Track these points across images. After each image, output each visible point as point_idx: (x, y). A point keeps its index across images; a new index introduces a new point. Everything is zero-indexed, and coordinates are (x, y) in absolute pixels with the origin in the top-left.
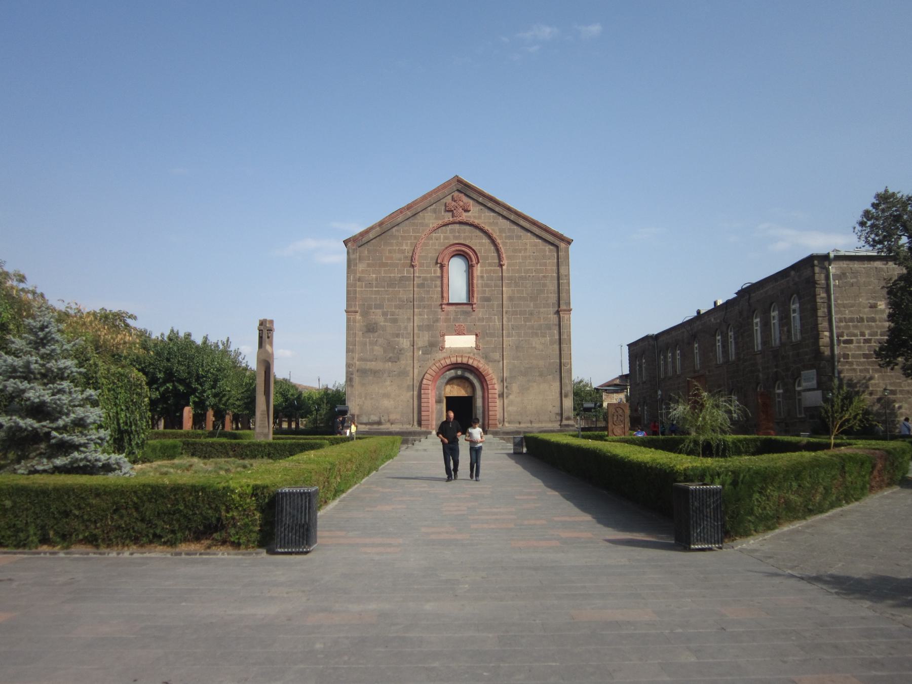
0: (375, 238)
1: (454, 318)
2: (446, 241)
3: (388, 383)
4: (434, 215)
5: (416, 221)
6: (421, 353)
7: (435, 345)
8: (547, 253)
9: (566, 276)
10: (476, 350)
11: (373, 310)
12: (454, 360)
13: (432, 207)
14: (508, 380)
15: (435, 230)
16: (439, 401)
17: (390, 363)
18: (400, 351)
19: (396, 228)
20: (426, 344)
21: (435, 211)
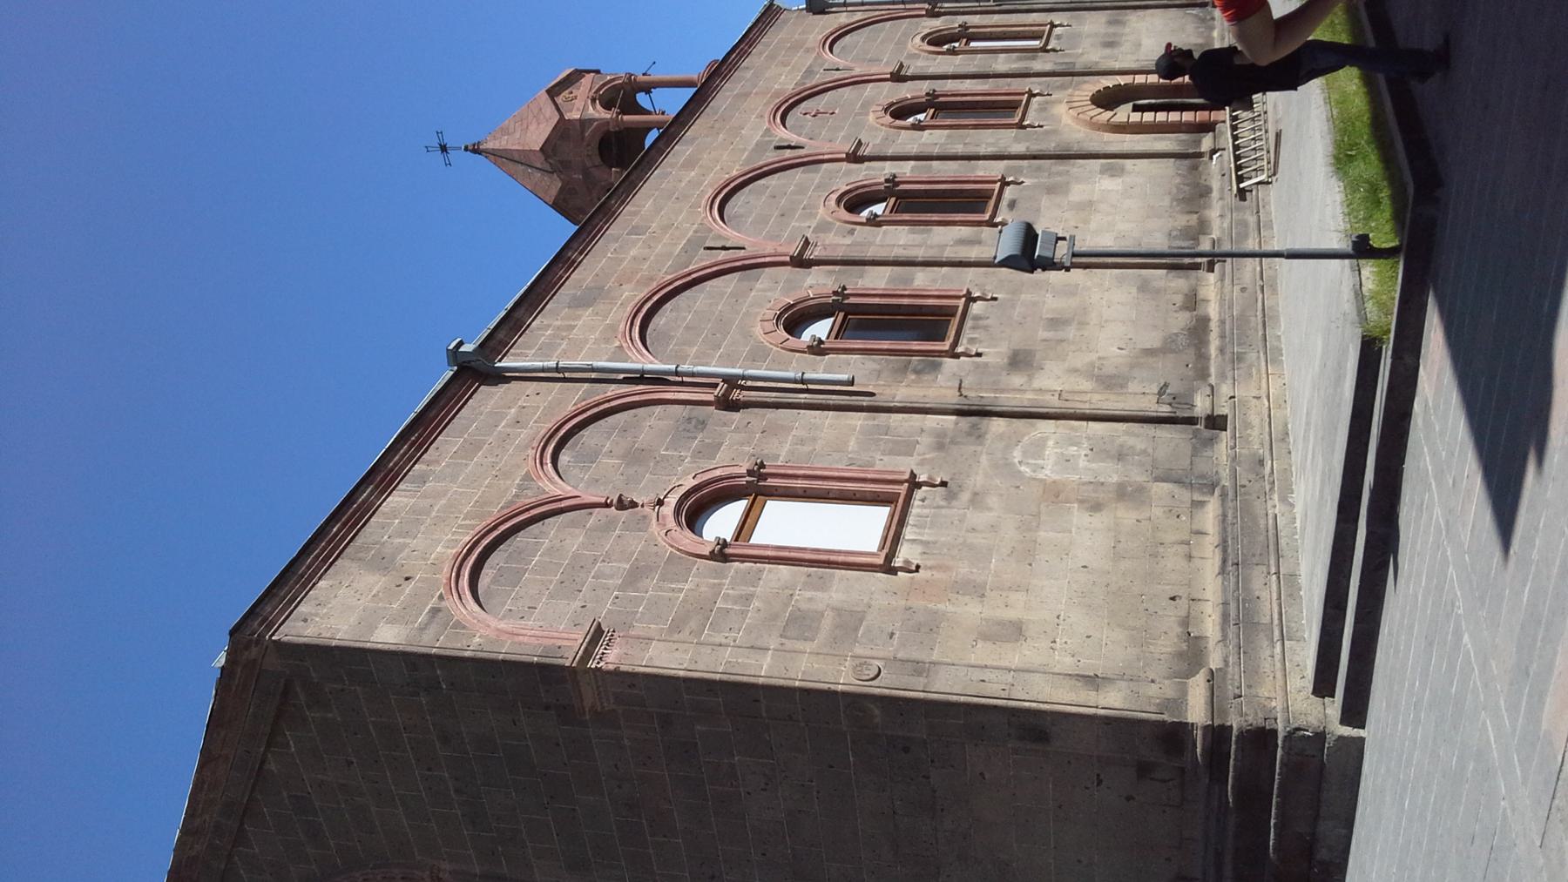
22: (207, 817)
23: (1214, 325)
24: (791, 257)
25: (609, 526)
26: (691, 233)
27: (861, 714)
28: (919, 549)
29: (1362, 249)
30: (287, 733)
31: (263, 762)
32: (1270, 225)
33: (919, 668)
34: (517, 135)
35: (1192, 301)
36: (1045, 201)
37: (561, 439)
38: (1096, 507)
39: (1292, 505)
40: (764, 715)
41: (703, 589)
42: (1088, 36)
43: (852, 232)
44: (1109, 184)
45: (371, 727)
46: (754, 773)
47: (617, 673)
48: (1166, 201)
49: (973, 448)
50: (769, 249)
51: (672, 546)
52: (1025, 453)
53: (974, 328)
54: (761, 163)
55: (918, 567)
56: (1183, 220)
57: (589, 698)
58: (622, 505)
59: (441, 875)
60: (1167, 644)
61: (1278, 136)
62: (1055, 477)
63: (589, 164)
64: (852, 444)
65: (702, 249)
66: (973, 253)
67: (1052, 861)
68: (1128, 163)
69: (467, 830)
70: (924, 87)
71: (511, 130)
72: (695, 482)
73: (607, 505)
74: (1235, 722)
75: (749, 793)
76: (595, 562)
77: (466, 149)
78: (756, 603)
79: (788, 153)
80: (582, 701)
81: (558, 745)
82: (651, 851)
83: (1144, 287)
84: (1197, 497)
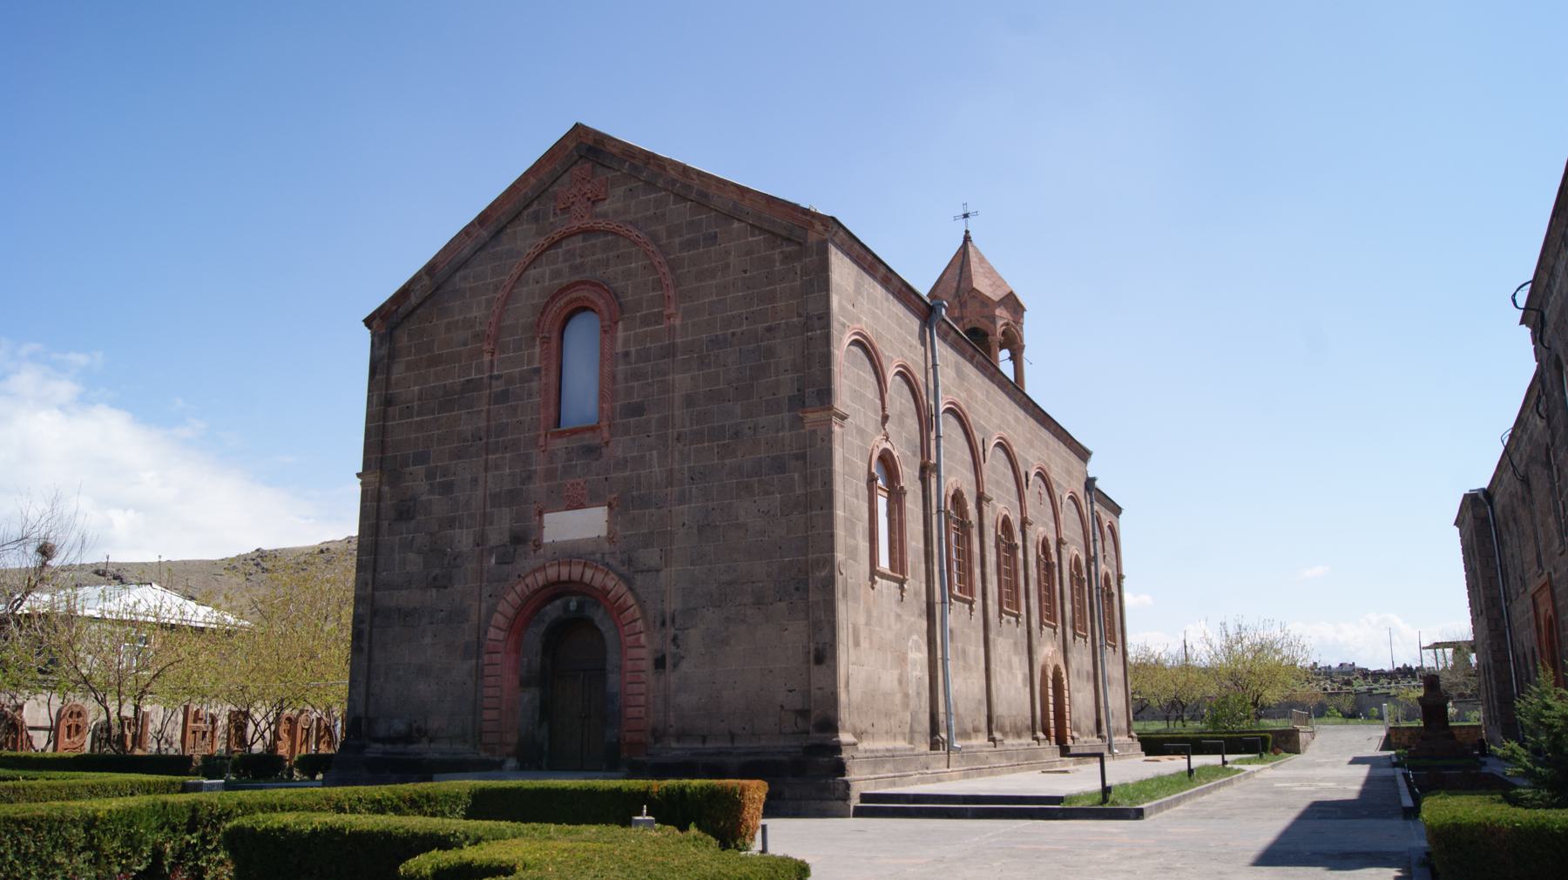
0: (420, 305)
1: (563, 467)
2: (555, 282)
3: (428, 640)
4: (534, 226)
5: (499, 249)
6: (493, 561)
7: (524, 538)
8: (778, 266)
9: (820, 318)
10: (607, 545)
11: (411, 468)
12: (552, 573)
13: (531, 210)
14: (678, 621)
15: (535, 261)
16: (525, 683)
17: (434, 590)
18: (455, 559)
19: (461, 273)
20: (506, 539)
21: (536, 218)
22: (697, 182)
23: (968, 743)
24: (983, 493)
25: (876, 412)
26: (988, 428)
27: (821, 565)
28: (880, 588)
29: (1106, 790)
30: (761, 237)
31: (739, 220)
32: (1014, 771)
33: (845, 595)
34: (981, 270)
35: (976, 730)
36: (1011, 641)
37: (905, 375)
38: (900, 682)
39: (916, 784)
40: (813, 513)
41: (859, 471)
42: (1081, 659)
43: (992, 526)
44: (1020, 677)
45: (773, 287)
46: (769, 505)
47: (830, 432)
48: (1015, 713)
49: (916, 612)
50: (985, 477)
51: (873, 450)
52: (916, 642)
53: (960, 606)
54: (1020, 464)
55: (873, 588)
56: (1007, 723)
57: (811, 416)
58: (885, 419)
59: (672, 319)
60: (863, 725)
61: (1066, 772)
62: (909, 659)
63: (965, 321)
64: (913, 543)
65: (982, 437)
66: (990, 602)
67: (733, 668)
68: (1028, 689)
69: (706, 337)
70: (1055, 559)
71: (983, 265)
72: (896, 457)
73: (883, 408)
74: (844, 755)
75: (755, 502)
76: (864, 408)
77: (967, 232)
78: (855, 501)
79: (1024, 480)
80: (812, 412)
81: (774, 394)
82: (706, 444)
83: (980, 701)
84: (907, 736)
